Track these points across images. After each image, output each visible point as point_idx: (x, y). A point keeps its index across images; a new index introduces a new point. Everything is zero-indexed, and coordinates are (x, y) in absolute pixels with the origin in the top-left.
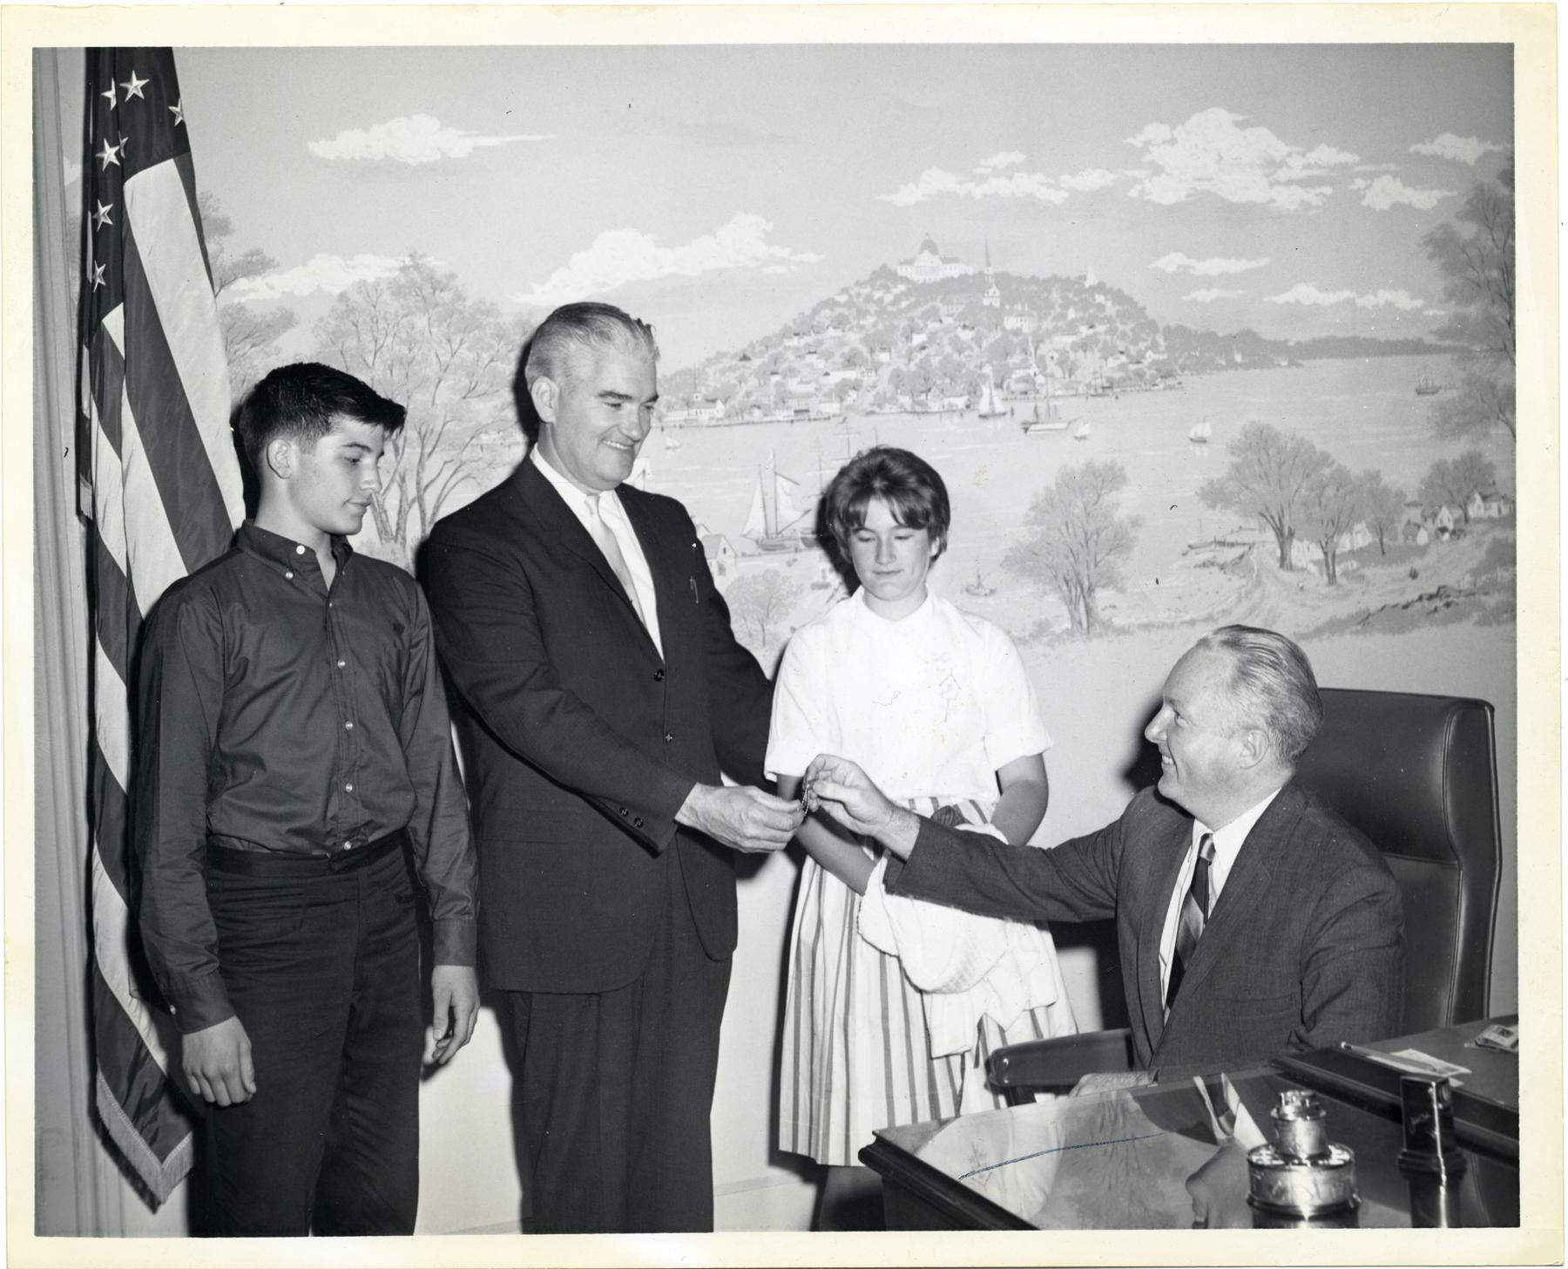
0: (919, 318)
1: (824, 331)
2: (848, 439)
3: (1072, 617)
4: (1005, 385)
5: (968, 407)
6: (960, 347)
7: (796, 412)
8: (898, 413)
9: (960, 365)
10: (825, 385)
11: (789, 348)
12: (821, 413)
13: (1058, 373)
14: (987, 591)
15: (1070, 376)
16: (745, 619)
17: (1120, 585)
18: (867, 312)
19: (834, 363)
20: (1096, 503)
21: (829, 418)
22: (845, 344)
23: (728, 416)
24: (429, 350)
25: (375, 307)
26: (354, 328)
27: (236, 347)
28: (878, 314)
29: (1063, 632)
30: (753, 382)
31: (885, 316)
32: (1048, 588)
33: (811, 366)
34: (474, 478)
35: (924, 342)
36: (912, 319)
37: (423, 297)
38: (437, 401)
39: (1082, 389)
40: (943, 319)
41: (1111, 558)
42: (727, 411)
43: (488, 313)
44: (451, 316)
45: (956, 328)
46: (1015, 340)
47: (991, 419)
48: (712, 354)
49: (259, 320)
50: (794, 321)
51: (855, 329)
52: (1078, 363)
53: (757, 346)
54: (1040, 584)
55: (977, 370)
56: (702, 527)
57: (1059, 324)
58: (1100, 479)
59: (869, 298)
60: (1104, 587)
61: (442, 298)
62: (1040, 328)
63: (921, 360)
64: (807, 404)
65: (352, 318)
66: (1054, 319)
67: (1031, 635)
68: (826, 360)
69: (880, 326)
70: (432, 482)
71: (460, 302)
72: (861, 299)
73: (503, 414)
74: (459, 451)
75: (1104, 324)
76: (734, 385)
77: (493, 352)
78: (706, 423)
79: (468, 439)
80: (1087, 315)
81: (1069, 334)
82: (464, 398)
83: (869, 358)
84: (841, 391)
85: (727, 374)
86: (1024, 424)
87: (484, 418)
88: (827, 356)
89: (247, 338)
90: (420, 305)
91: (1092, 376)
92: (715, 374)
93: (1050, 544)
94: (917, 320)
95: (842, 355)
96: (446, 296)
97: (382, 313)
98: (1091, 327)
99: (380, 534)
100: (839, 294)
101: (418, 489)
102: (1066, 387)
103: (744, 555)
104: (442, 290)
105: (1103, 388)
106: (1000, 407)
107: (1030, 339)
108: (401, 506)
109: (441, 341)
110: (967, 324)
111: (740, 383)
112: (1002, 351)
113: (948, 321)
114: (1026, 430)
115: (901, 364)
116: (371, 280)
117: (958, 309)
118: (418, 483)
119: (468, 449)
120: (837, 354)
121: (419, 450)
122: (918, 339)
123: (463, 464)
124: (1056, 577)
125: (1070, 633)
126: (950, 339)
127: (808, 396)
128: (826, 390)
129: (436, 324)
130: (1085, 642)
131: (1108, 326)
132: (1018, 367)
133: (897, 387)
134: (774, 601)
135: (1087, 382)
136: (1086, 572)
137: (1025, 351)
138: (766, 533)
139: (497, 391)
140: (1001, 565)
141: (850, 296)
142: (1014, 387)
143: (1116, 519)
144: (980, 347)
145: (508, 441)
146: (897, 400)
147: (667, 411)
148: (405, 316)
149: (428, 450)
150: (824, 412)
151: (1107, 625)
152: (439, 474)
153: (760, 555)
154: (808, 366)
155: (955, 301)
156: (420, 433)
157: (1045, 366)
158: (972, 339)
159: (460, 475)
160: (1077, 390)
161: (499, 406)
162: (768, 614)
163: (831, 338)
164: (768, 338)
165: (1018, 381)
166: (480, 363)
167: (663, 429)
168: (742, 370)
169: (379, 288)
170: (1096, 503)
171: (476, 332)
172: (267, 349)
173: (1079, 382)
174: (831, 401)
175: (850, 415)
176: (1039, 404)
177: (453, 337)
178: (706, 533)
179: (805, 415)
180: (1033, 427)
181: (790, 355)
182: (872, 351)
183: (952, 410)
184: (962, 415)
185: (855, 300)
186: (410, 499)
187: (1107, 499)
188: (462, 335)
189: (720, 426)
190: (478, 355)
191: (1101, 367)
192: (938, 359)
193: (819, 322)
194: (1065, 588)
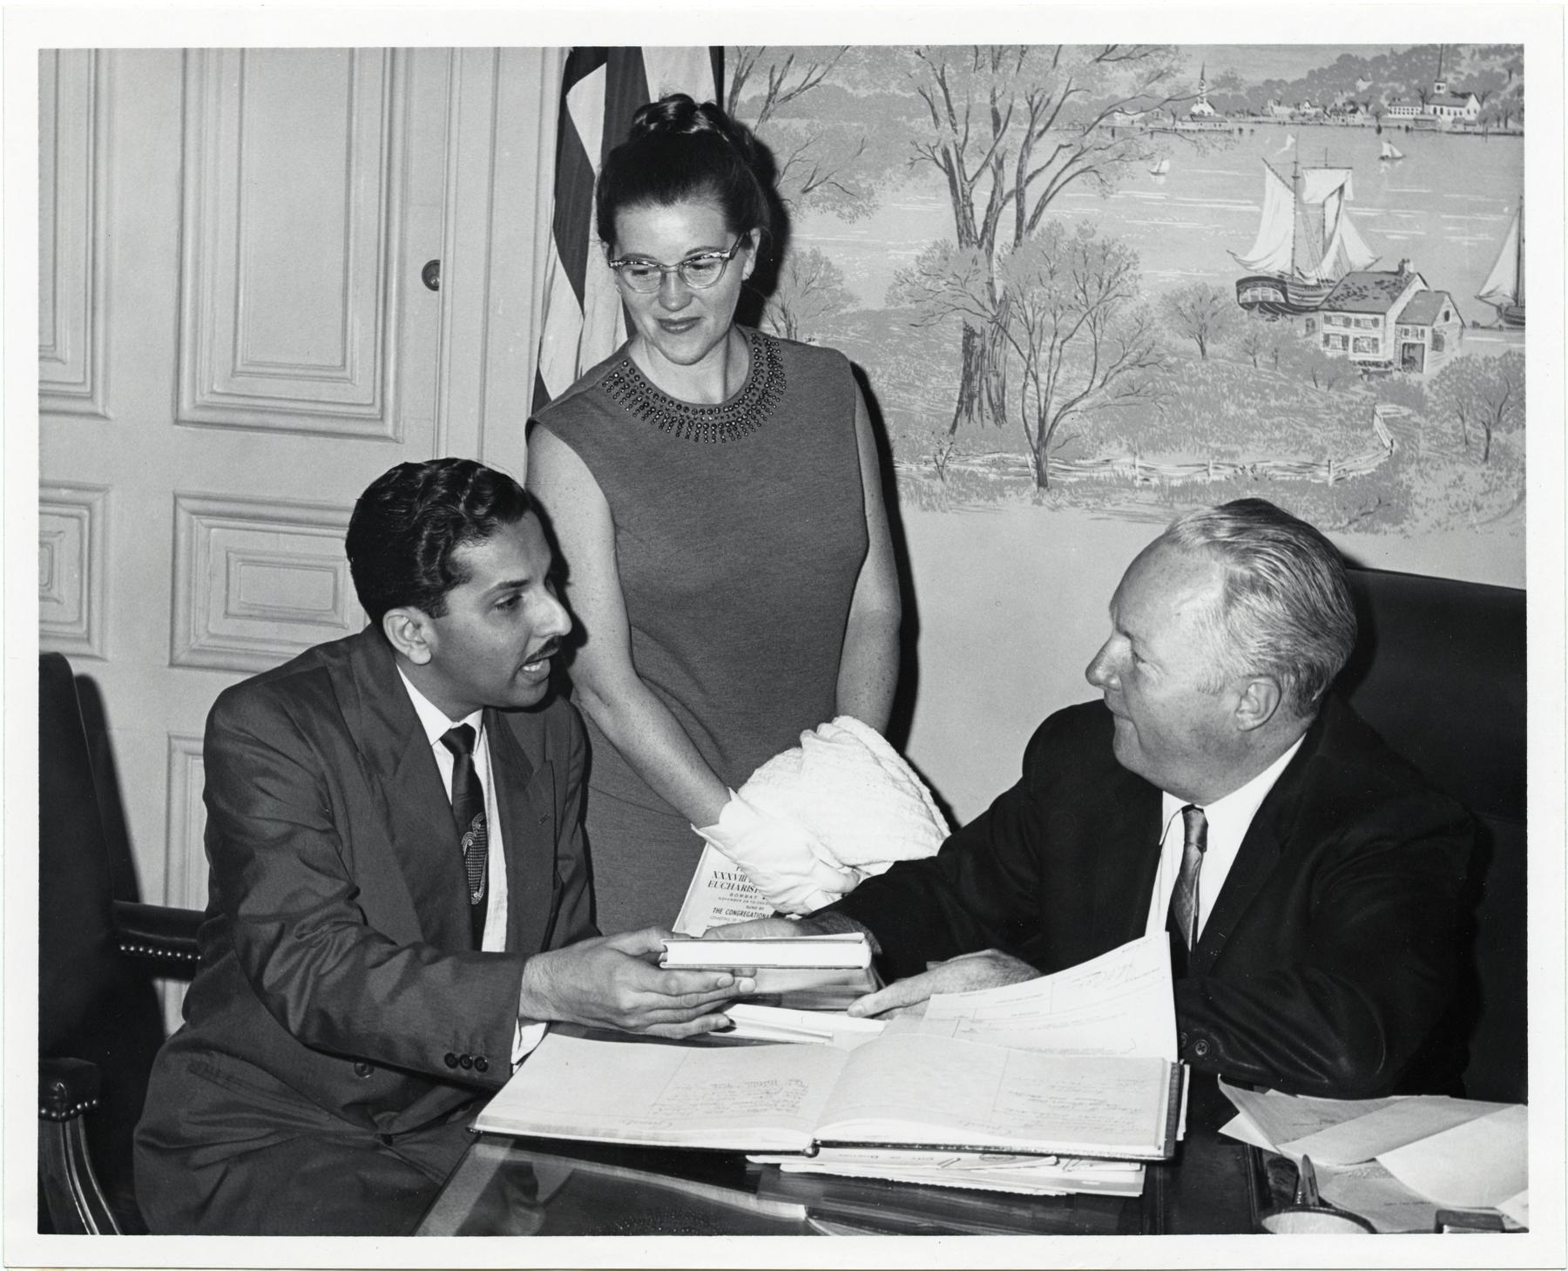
16: (1462, 418)
23: (1483, 120)
34: (1095, 171)
38: (1061, 62)
42: (1481, 113)
56: (1418, 277)
70: (1038, 171)
73: (1149, 87)
74: (1082, 133)
76: (1504, 76)
78: (1446, 128)
79: (1095, 119)
82: (1098, 60)
85: (1492, 57)
87: (1123, 92)
99: (960, 236)
101: (1019, 181)
103: (1475, 325)
108: (992, 200)
111: (1510, 73)
118: (1020, 172)
119: (1093, 132)
121: (1027, 126)
123: (1083, 151)
134: (1511, 398)
138: (1516, 301)
139: (1145, 55)
145: (1151, 125)
147: (1390, 105)
149: (1039, 127)
152: (1049, 162)
153: (1501, 327)
156: (1031, 104)
159: (1077, 166)
161: (1146, 76)
162: (1499, 414)
167: (1379, 130)
168: (1516, 54)
178: (1426, 288)
186: (1006, 191)
189: (1468, 133)
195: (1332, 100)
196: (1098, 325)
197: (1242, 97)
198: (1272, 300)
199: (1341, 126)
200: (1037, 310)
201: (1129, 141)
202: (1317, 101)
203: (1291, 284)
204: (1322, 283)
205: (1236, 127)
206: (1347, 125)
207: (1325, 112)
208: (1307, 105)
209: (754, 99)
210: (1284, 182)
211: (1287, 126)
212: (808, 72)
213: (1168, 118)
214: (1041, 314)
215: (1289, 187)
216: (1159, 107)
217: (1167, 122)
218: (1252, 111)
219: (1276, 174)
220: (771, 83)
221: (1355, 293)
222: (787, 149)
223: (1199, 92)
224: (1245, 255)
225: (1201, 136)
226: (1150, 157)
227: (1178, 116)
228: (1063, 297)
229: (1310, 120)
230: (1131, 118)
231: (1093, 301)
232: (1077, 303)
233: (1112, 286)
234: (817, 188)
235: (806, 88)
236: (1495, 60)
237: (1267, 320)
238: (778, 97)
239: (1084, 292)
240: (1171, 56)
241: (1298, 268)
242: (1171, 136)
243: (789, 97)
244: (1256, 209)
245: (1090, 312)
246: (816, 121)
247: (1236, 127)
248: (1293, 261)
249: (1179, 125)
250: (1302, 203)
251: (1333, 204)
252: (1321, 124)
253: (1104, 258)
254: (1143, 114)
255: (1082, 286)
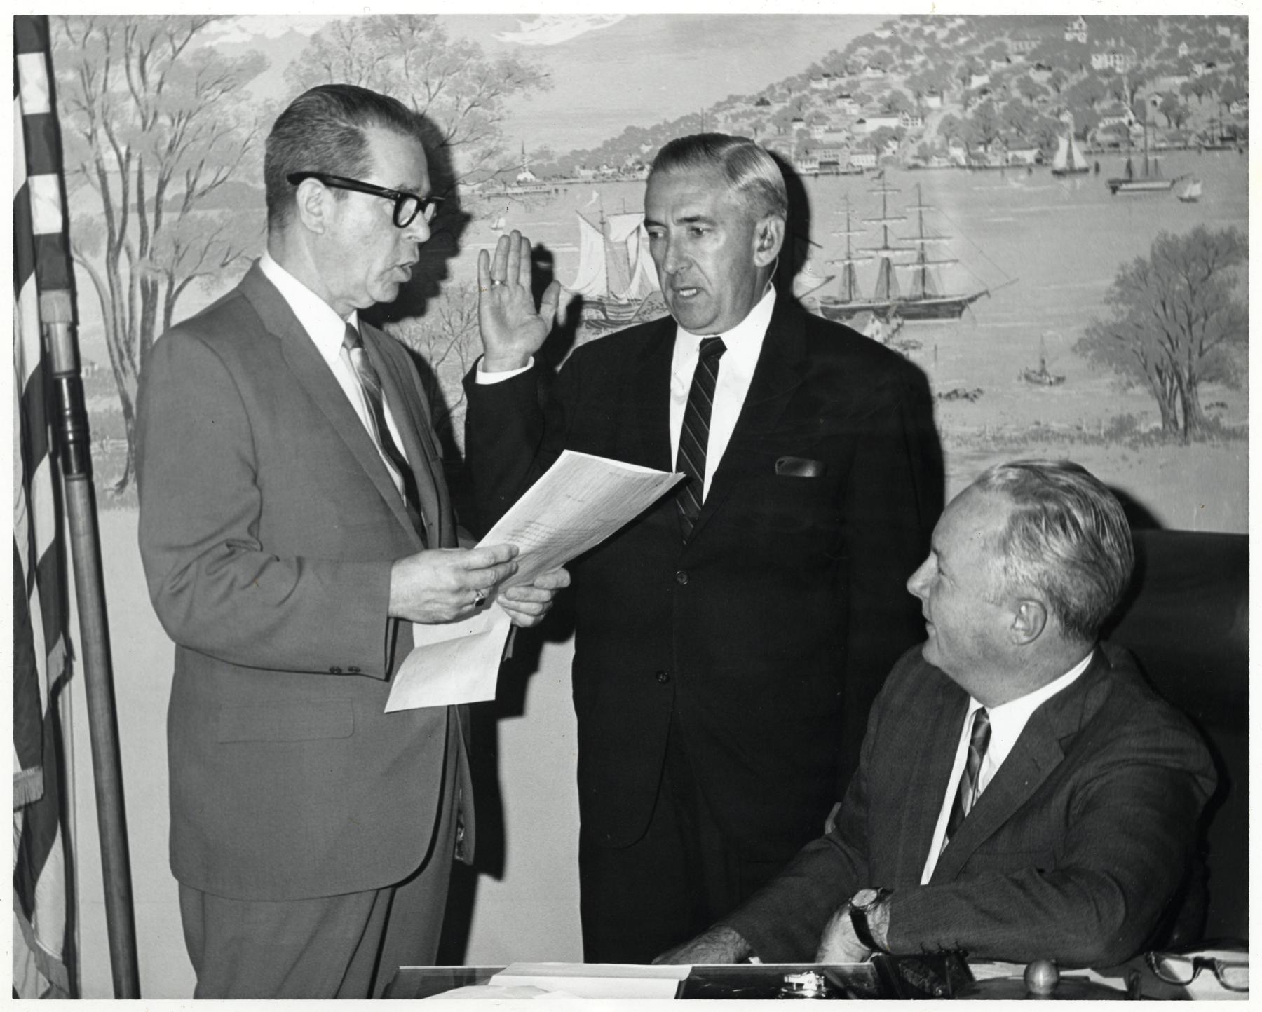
0: (981, 56)
1: (861, 72)
2: (884, 196)
3: (1164, 415)
4: (1089, 136)
5: (1039, 161)
6: (1030, 90)
7: (821, 164)
8: (947, 167)
9: (1031, 112)
10: (858, 134)
11: (815, 91)
12: (853, 166)
13: (1162, 120)
14: (1053, 379)
15: (1178, 125)
17: (1233, 378)
18: (916, 49)
19: (871, 109)
20: (1205, 279)
21: (861, 172)
22: (887, 87)
24: (406, 94)
25: (349, 48)
26: (326, 71)
27: (207, 92)
28: (928, 52)
29: (1151, 432)
30: (771, 128)
31: (938, 55)
32: (1134, 379)
33: (844, 110)
35: (985, 85)
36: (971, 59)
37: (401, 37)
39: (1192, 141)
40: (1010, 58)
41: (1222, 346)
43: (469, 54)
44: (430, 57)
45: (1027, 68)
46: (1105, 82)
47: (1068, 176)
48: (723, 98)
49: (229, 64)
50: (824, 61)
51: (900, 70)
52: (1190, 110)
53: (777, 89)
54: (1124, 374)
55: (1055, 118)
57: (1169, 62)
58: (1212, 251)
59: (918, 34)
60: (1210, 380)
61: (420, 38)
62: (1139, 67)
63: (981, 105)
64: (834, 156)
65: (325, 61)
66: (1157, 58)
67: (1105, 434)
68: (862, 105)
69: (931, 66)
71: (440, 43)
72: (908, 35)
73: (483, 163)
75: (1229, 62)
77: (474, 96)
80: (1204, 51)
81: (1179, 75)
83: (915, 104)
84: (878, 142)
85: (741, 120)
86: (1110, 182)
88: (863, 100)
89: (217, 82)
90: (397, 45)
91: (1208, 125)
92: (727, 118)
93: (1138, 326)
94: (978, 59)
95: (881, 100)
96: (425, 36)
97: (357, 55)
98: (1210, 65)
100: (881, 29)
102: (1172, 139)
104: (421, 30)
105: (1223, 139)
106: (1080, 162)
107: (1125, 80)
109: (416, 87)
110: (1043, 63)
111: (756, 130)
112: (1088, 95)
113: (1019, 60)
114: (1114, 190)
115: (955, 110)
116: (345, 21)
117: (1030, 46)
120: (875, 98)
122: (977, 82)
124: (1145, 366)
125: (1161, 435)
126: (1018, 81)
127: (838, 146)
128: (859, 139)
129: (414, 66)
130: (1180, 445)
131: (1233, 64)
132: (1107, 114)
133: (948, 138)
135: (1200, 132)
136: (1187, 362)
137: (1118, 96)
139: (477, 139)
140: (1074, 350)
141: (894, 31)
142: (1100, 137)
143: (1232, 299)
144: (1058, 90)
146: (948, 153)
148: (381, 58)
150: (855, 164)
151: (1213, 428)
154: (838, 111)
155: (1028, 37)
157: (1144, 114)
158: (1049, 81)
160: (1186, 142)
161: (480, 155)
163: (869, 79)
164: (789, 79)
165: (1106, 131)
166: (460, 108)
168: (759, 116)
169: (354, 29)
170: (1205, 279)
171: (457, 74)
172: (237, 94)
173: (1190, 133)
174: (866, 153)
175: (889, 169)
176: (1133, 158)
177: (430, 81)
179: (833, 169)
180: (1124, 186)
181: (817, 99)
182: (919, 96)
183: (1017, 165)
184: (1030, 171)
185: (900, 36)
187: (1220, 275)
188: (441, 78)
190: (457, 98)
191: (1221, 114)
192: (1002, 104)
193: (854, 62)
194: (1157, 379)
195: (624, 162)
196: (463, 348)
197: (554, 165)
198: (595, 318)
199: (633, 181)
200: (414, 342)
201: (472, 205)
202: (612, 163)
203: (609, 305)
204: (632, 302)
205: (552, 188)
206: (637, 180)
207: (619, 172)
208: (605, 167)
209: (175, 198)
210: (594, 227)
211: (591, 186)
212: (216, 173)
213: (500, 185)
214: (418, 344)
215: (598, 230)
216: (492, 177)
217: (500, 188)
218: (564, 175)
219: (588, 222)
220: (188, 183)
221: (658, 308)
222: (206, 234)
223: (521, 163)
224: (571, 285)
225: (527, 197)
226: (489, 217)
227: (508, 183)
228: (434, 329)
229: (608, 178)
230: (471, 188)
231: (457, 331)
232: (445, 333)
233: (471, 317)
234: (232, 263)
235: (216, 185)
236: (743, 122)
237: (594, 334)
238: (196, 193)
239: (449, 324)
240: (498, 138)
241: (612, 292)
242: (503, 199)
243: (203, 193)
244: (575, 249)
245: (456, 339)
246: (227, 210)
247: (552, 188)
248: (608, 287)
249: (509, 191)
250: (610, 242)
251: (633, 242)
252: (617, 181)
253: (463, 297)
254: (480, 185)
255: (447, 319)
